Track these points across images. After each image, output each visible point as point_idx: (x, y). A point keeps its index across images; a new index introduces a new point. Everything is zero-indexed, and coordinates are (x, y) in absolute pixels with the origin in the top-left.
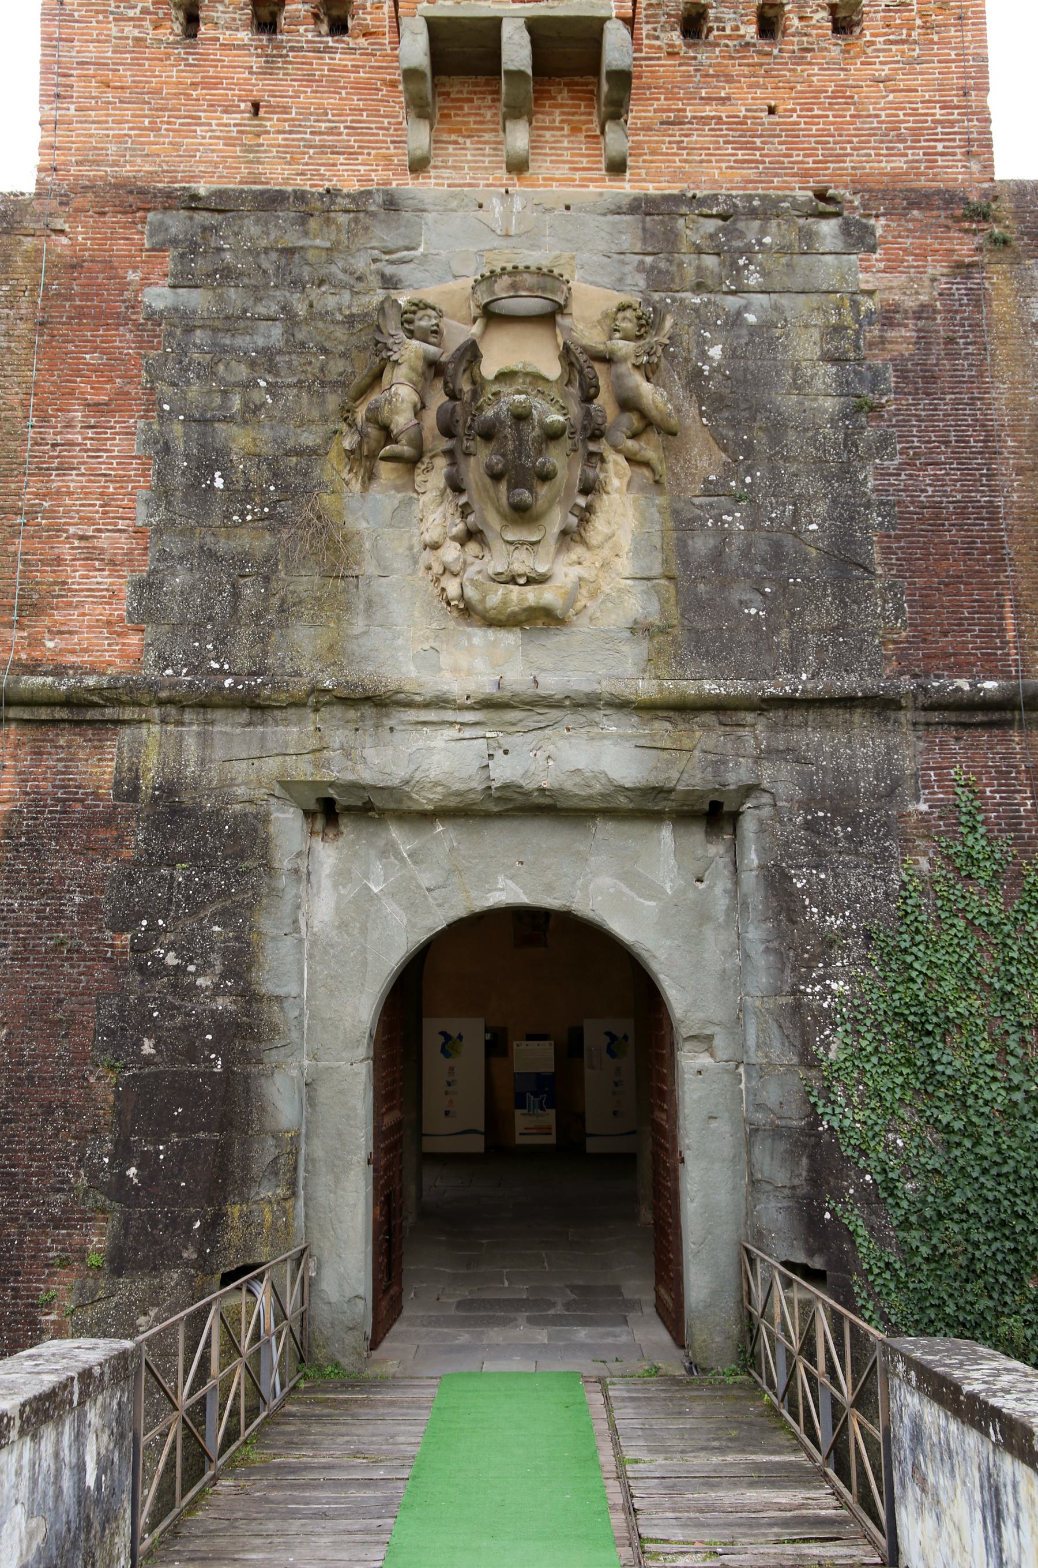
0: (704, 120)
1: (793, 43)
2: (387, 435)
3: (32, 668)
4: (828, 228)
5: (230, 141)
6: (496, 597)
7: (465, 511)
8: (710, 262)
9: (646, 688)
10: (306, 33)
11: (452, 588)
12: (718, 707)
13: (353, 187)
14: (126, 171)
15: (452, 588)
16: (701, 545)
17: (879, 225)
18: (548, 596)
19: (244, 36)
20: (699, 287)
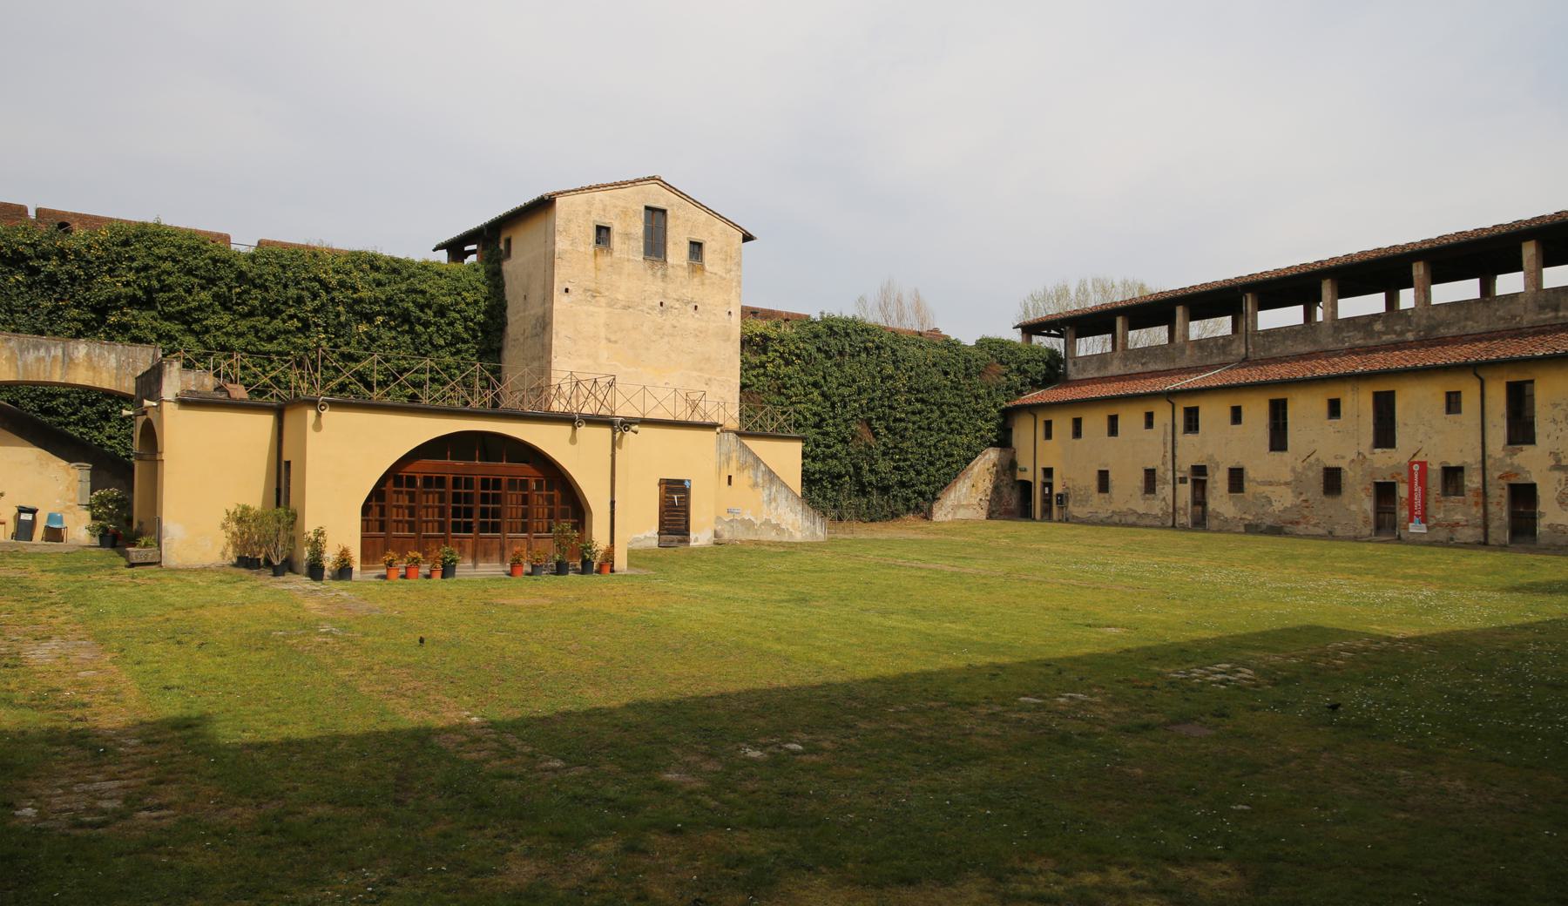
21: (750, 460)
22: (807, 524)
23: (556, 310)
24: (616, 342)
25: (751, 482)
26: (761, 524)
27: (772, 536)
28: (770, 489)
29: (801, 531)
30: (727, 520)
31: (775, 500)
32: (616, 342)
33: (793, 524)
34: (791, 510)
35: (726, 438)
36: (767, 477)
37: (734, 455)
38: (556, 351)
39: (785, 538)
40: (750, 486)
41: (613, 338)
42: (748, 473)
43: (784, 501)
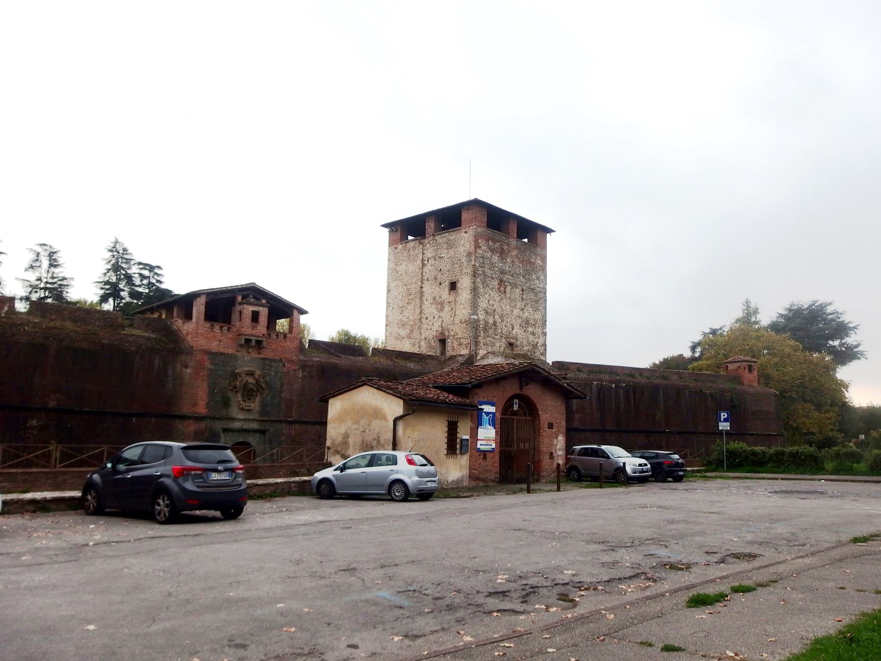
0: (269, 348)
1: (279, 339)
2: (235, 388)
3: (195, 413)
4: (281, 364)
5: (217, 345)
6: (246, 408)
7: (244, 398)
8: (268, 367)
9: (259, 418)
10: (226, 331)
11: (241, 406)
12: (266, 421)
13: (230, 353)
14: (205, 348)
15: (241, 406)
16: (265, 402)
17: (286, 364)
18: (251, 408)
19: (219, 331)
20: (267, 370)
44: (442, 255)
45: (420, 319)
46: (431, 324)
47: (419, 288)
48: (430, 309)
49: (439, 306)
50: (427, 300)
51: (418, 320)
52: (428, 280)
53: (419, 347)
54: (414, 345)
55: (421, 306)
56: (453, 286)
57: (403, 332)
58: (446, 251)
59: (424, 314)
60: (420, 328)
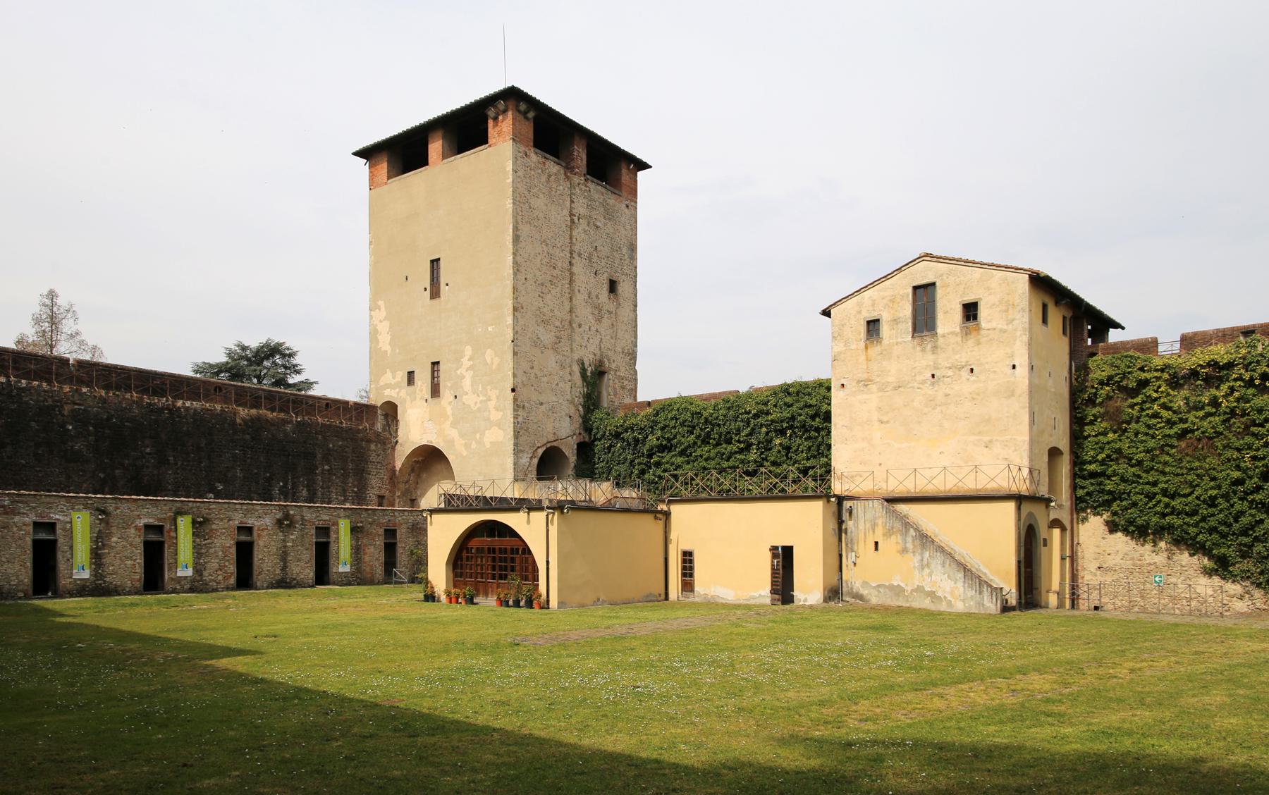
21: (898, 525)
22: (971, 593)
23: (834, 405)
24: (888, 422)
25: (899, 547)
26: (912, 591)
27: (926, 604)
28: (922, 554)
29: (963, 601)
30: (874, 585)
31: (928, 565)
32: (888, 422)
33: (952, 593)
34: (949, 577)
35: (871, 506)
36: (918, 542)
37: (880, 522)
38: (835, 441)
39: (943, 607)
40: (898, 552)
41: (885, 419)
42: (896, 539)
43: (940, 567)
44: (598, 224)
45: (571, 323)
46: (586, 337)
47: (568, 263)
48: (584, 313)
49: (596, 312)
50: (579, 291)
51: (567, 323)
52: (580, 255)
53: (570, 374)
54: (563, 367)
55: (571, 298)
56: (613, 286)
57: (547, 337)
58: (603, 220)
59: (576, 316)
60: (570, 337)
